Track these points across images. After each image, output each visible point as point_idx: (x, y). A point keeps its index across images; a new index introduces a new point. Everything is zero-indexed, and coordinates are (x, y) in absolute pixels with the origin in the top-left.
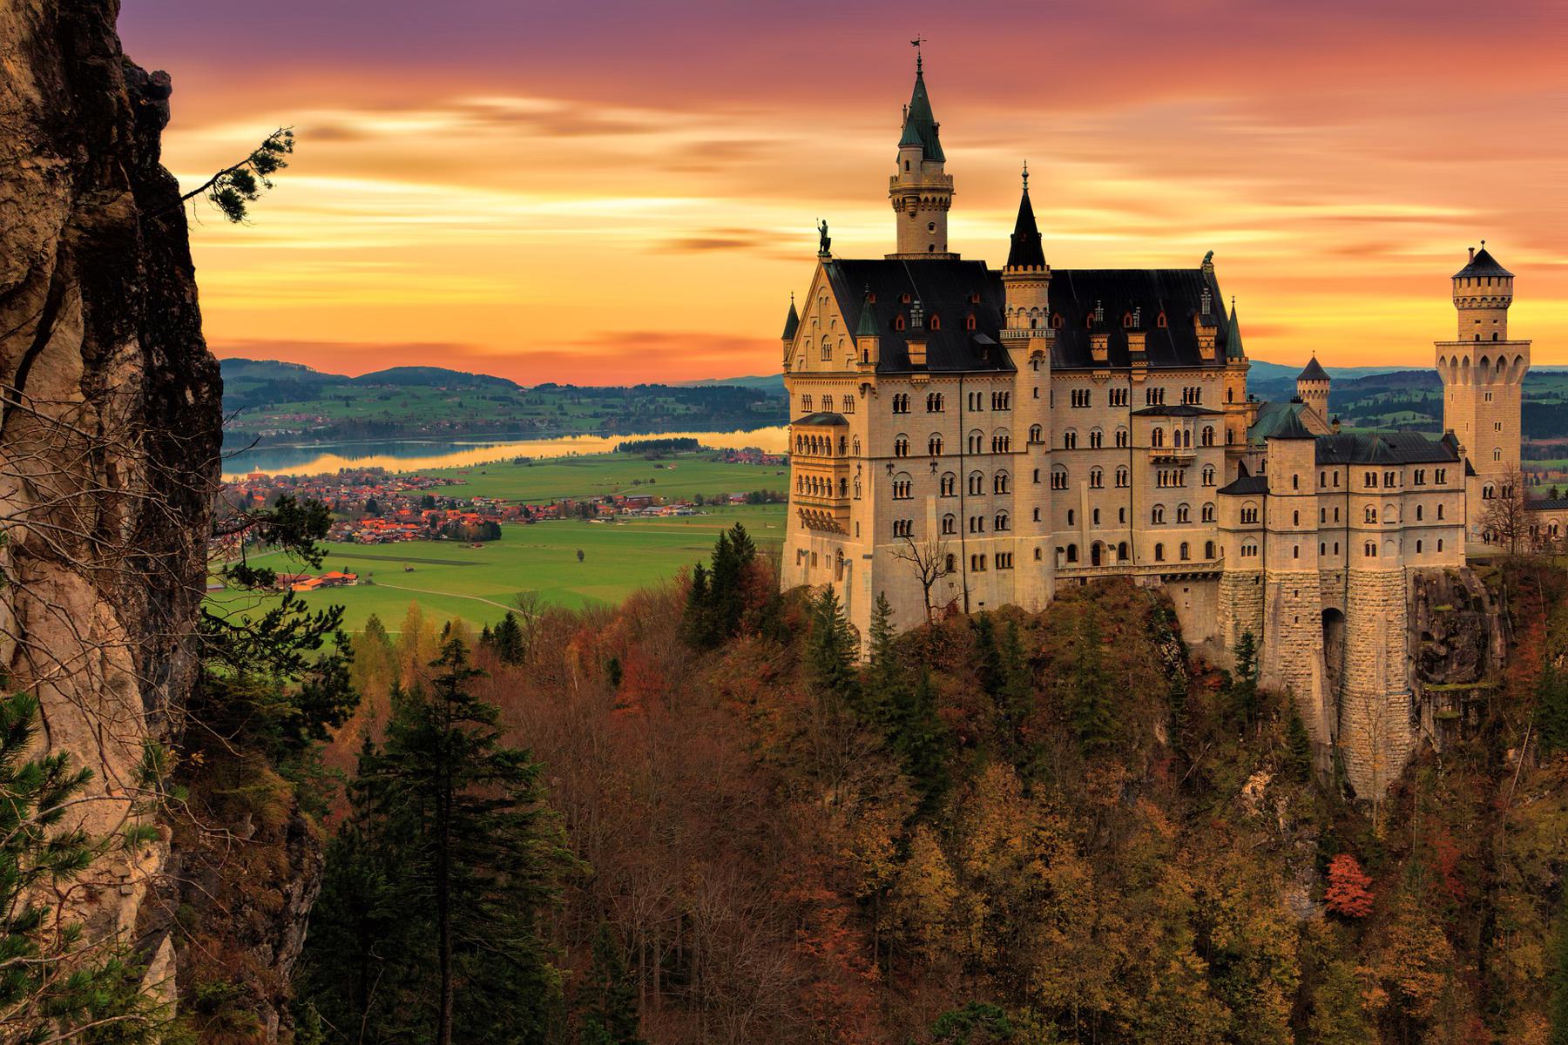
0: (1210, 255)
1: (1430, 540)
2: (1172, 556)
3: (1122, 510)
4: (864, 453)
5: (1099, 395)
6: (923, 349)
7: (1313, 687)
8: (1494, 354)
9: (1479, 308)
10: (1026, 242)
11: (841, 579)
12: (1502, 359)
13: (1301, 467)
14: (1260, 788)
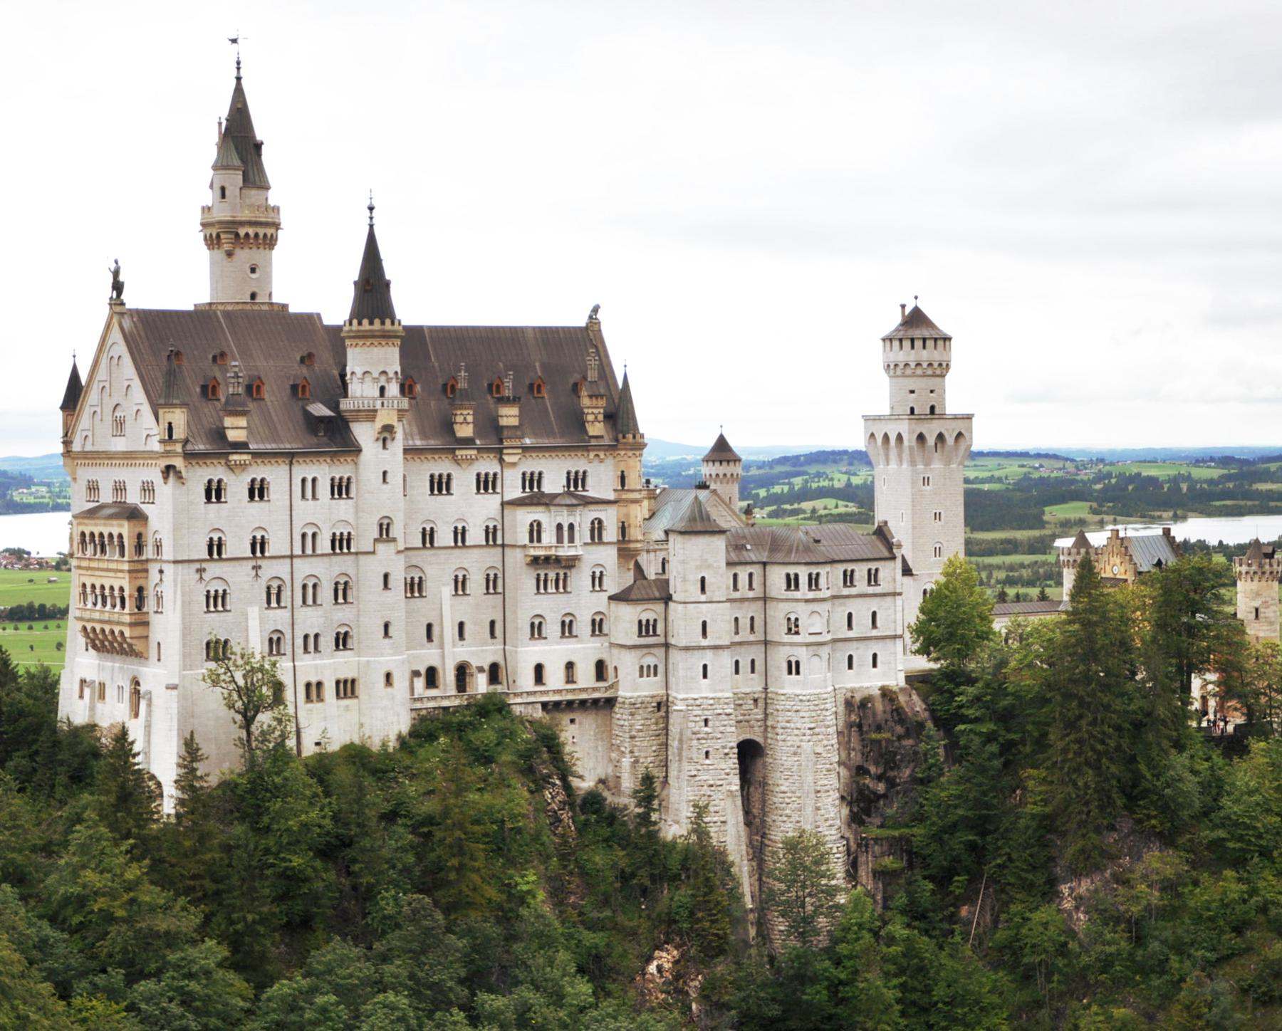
0: (596, 310)
1: (862, 654)
2: (554, 678)
3: (492, 623)
4: (167, 553)
5: (463, 480)
6: (242, 422)
7: (729, 834)
8: (931, 430)
9: (914, 375)
11: (136, 715)
12: (941, 437)
13: (709, 566)
14: (667, 966)
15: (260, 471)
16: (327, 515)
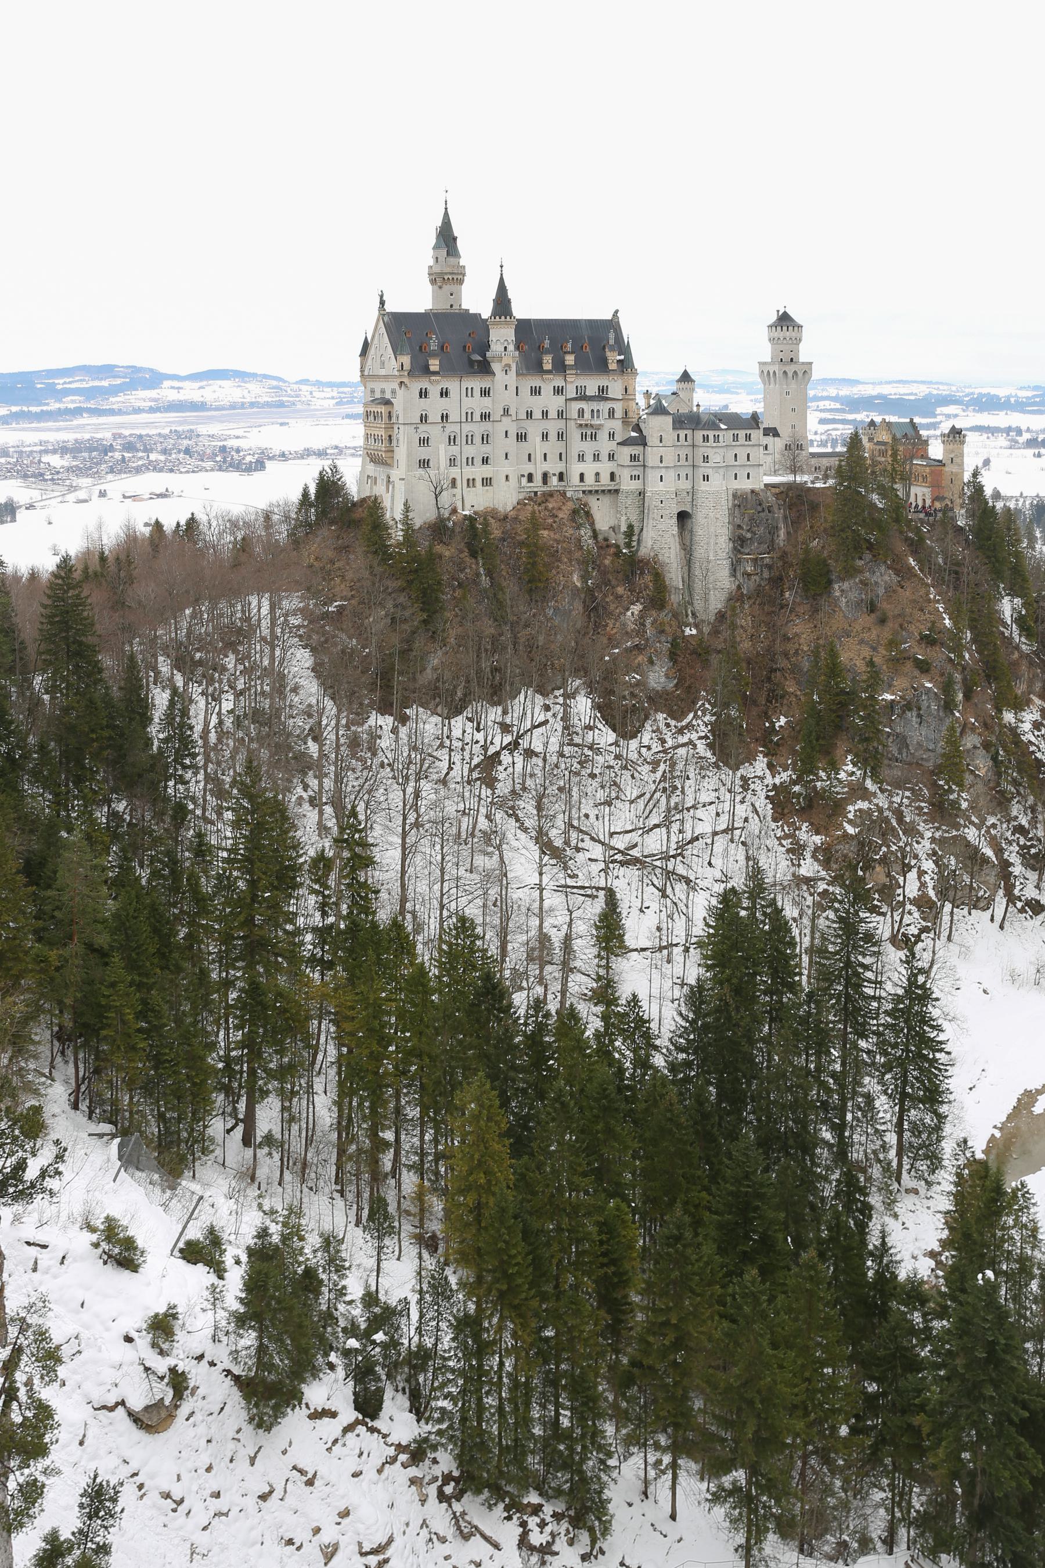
10: (502, 304)
15: (445, 384)
16: (478, 404)
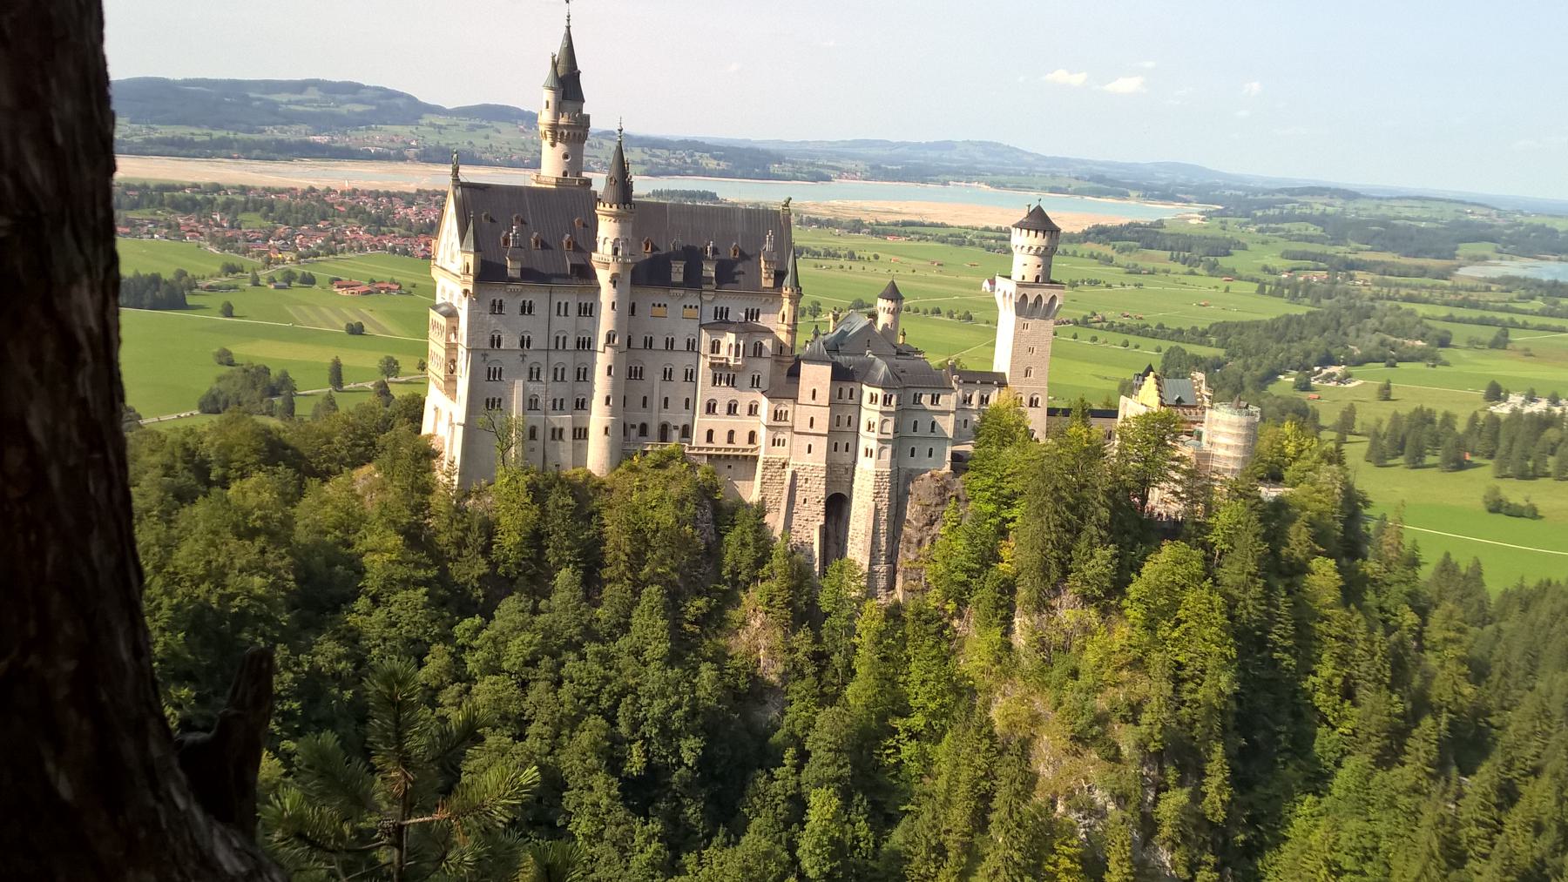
2: (720, 440)
